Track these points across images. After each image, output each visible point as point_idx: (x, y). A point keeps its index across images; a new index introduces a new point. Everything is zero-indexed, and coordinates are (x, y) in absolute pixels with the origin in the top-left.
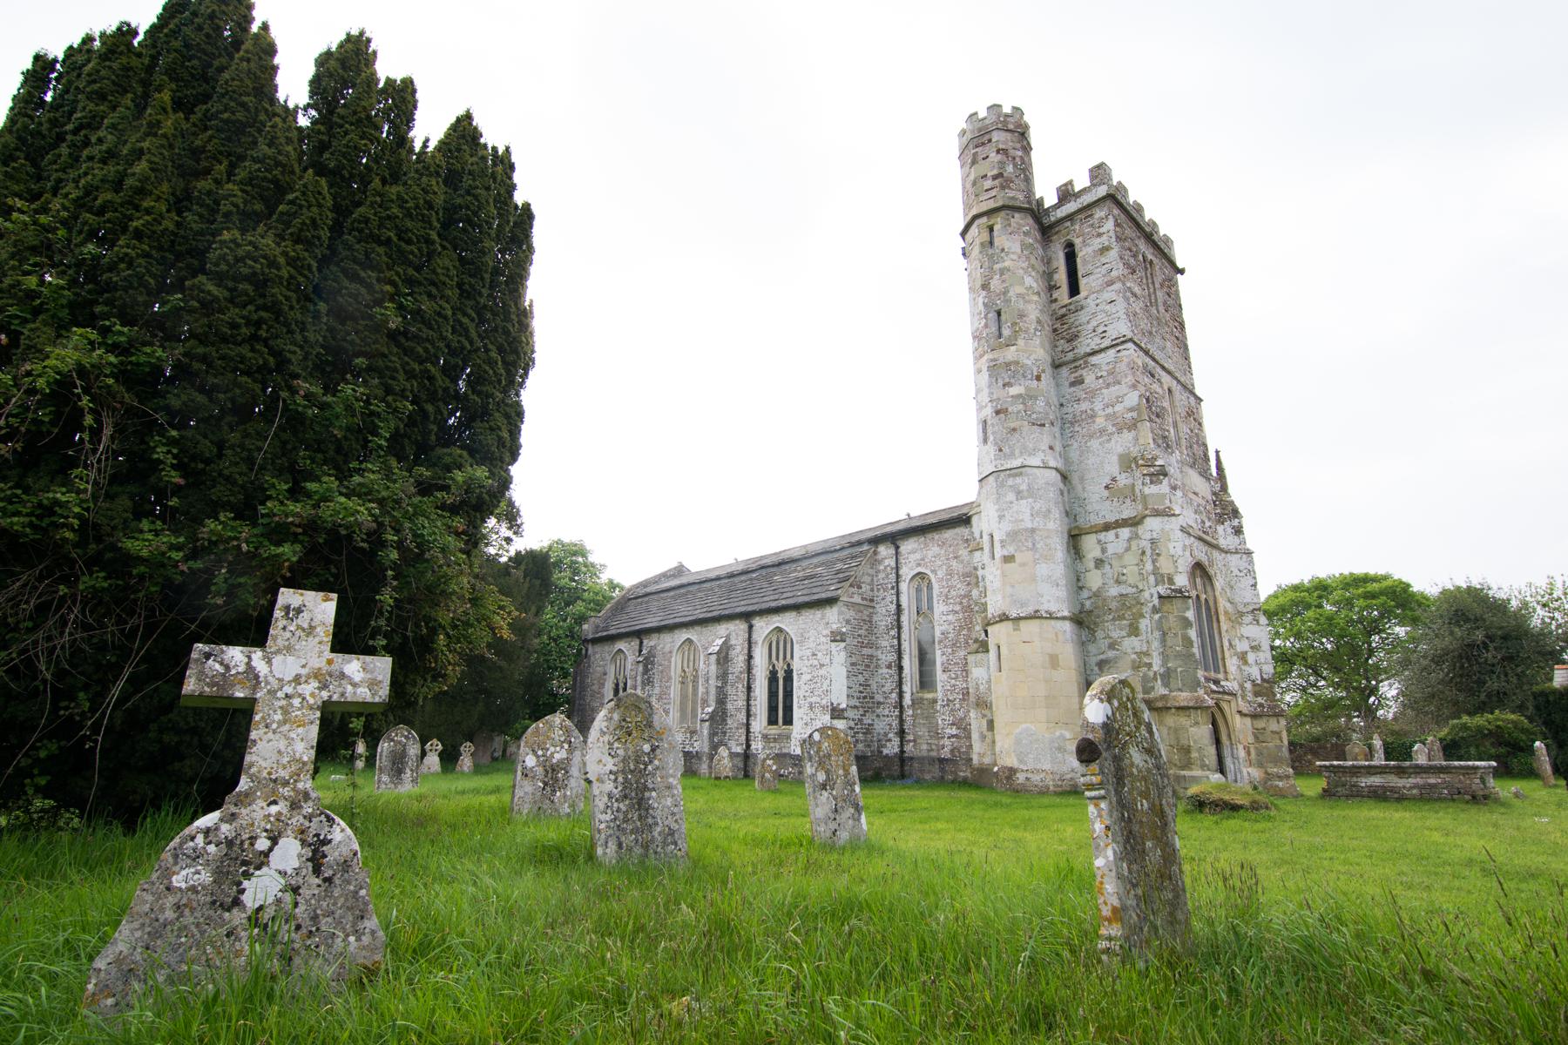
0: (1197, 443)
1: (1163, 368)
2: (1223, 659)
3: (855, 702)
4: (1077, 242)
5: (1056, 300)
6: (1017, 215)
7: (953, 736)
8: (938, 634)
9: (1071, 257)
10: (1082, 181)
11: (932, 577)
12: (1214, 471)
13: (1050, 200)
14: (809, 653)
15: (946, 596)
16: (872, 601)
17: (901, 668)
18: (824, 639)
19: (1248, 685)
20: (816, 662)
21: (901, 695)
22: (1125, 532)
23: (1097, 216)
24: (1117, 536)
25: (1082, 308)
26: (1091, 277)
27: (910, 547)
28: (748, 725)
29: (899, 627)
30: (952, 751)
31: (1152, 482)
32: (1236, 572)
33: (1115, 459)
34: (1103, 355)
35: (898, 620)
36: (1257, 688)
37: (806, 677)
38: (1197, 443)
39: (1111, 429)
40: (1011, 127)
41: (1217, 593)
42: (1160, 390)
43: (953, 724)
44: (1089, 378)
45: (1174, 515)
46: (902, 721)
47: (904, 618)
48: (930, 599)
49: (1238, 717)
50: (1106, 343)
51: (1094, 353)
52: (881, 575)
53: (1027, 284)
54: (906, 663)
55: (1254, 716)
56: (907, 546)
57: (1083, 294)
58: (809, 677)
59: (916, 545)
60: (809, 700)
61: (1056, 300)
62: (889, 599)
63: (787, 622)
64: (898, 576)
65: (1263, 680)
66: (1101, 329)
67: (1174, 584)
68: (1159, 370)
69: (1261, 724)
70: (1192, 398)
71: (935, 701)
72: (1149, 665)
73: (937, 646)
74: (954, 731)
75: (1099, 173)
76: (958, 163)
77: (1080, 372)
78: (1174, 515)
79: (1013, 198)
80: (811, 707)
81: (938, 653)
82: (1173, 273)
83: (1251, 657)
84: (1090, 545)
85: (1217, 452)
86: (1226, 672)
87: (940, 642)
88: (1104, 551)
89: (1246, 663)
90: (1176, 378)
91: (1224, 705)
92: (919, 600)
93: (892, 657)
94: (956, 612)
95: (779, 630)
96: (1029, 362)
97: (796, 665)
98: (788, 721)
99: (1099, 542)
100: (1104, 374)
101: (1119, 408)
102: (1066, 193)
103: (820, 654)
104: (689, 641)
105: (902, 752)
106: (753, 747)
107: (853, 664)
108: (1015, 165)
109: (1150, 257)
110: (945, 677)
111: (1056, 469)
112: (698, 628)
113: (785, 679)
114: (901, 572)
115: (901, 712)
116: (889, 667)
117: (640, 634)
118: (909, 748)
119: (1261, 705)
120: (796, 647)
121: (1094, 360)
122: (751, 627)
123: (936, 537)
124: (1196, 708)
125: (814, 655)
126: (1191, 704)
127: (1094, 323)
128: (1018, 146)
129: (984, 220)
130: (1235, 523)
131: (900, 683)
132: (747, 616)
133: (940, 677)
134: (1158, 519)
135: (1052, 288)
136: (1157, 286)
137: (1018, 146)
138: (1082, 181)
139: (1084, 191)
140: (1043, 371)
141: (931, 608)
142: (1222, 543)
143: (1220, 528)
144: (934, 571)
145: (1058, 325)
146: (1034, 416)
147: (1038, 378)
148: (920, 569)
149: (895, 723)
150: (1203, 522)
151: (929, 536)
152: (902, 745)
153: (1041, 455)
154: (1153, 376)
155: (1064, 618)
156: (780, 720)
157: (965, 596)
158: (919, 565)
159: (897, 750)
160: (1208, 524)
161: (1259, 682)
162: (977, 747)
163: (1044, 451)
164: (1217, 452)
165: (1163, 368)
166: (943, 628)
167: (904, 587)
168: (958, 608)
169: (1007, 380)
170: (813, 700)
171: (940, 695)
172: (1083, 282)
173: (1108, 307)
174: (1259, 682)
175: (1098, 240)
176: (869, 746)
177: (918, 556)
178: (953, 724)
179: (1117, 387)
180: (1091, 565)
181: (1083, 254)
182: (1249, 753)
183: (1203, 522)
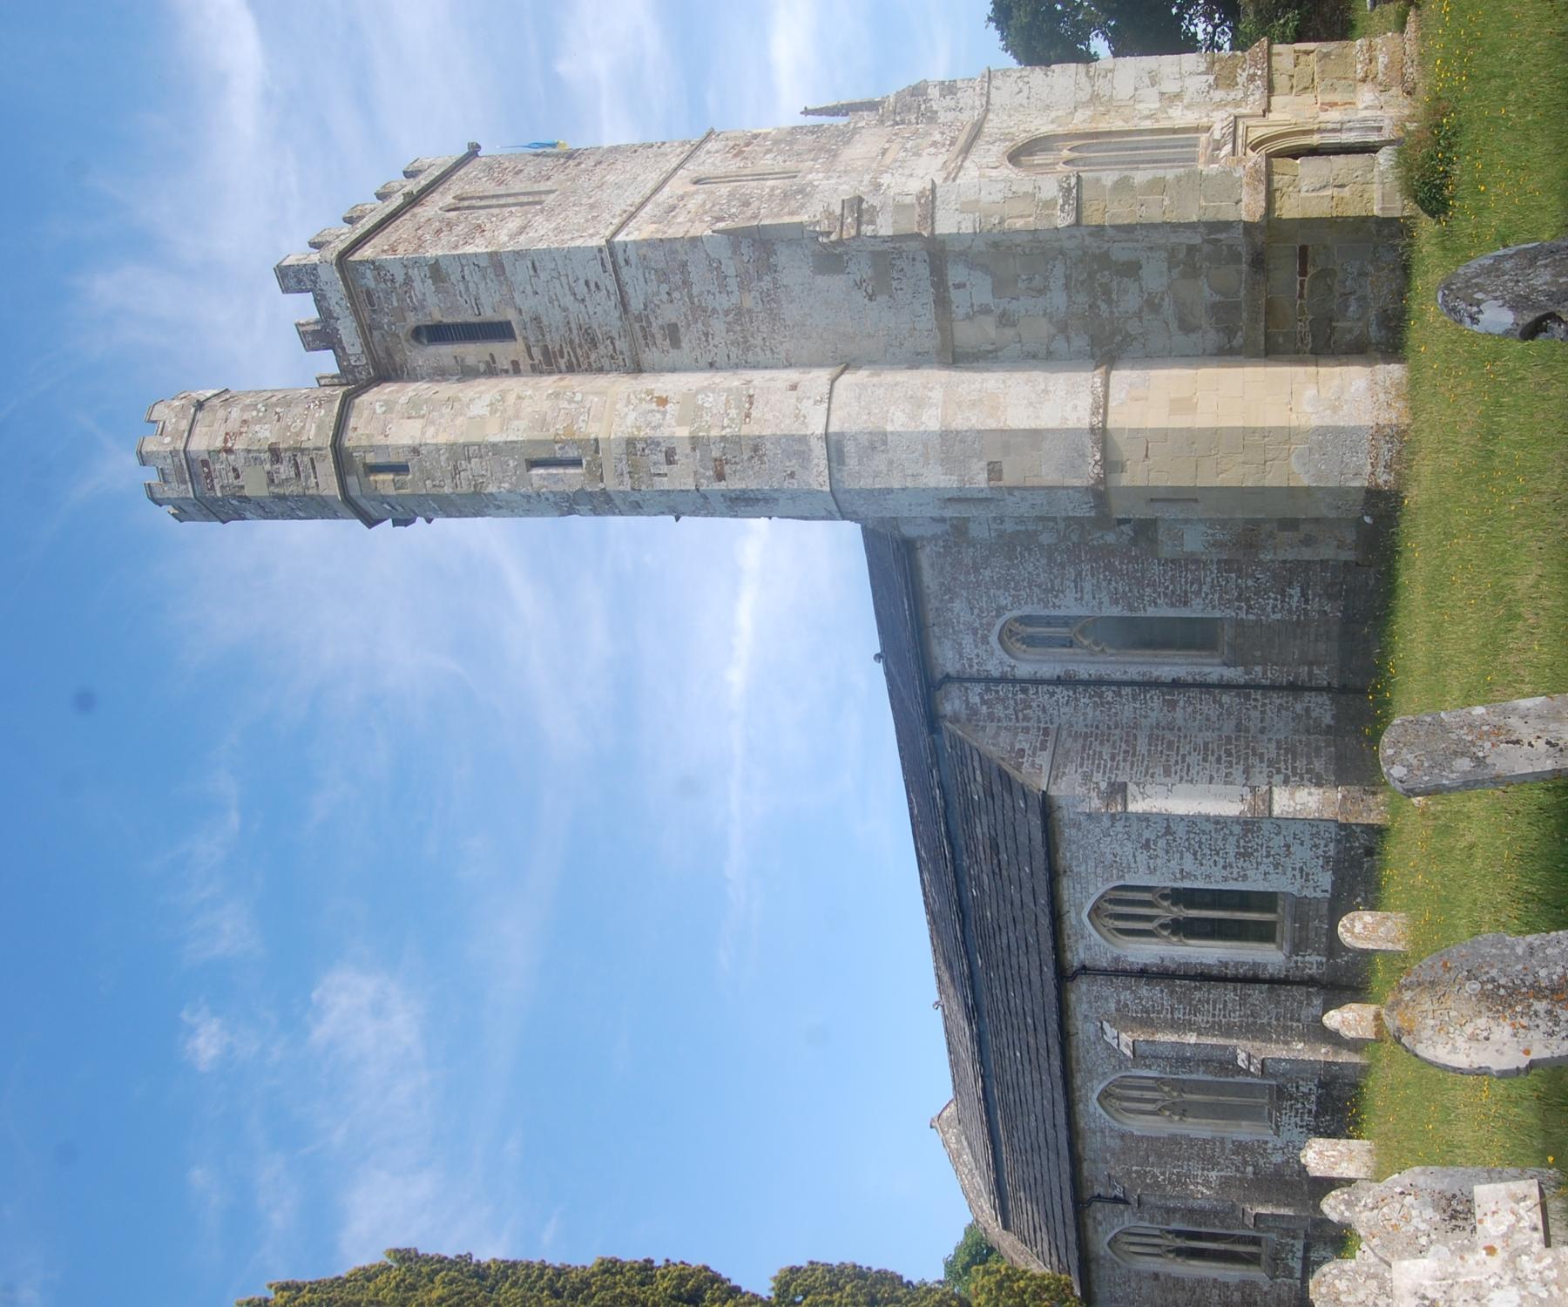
0: (790, 143)
1: (656, 190)
2: (1174, 131)
3: (1237, 771)
4: (413, 320)
5: (515, 364)
6: (352, 422)
7: (1304, 594)
8: (1115, 611)
9: (437, 333)
10: (303, 308)
11: (1008, 615)
12: (840, 121)
13: (327, 362)
14: (1142, 857)
15: (1046, 591)
16: (1046, 732)
17: (1176, 684)
19: (1218, 95)
20: (1162, 843)
21: (1226, 686)
22: (956, 273)
23: (372, 284)
24: (959, 286)
25: (537, 319)
26: (483, 300)
27: (950, 654)
28: (1273, 981)
29: (1099, 682)
30: (1330, 597)
31: (872, 222)
32: (1022, 98)
33: (822, 281)
34: (630, 290)
35: (1087, 683)
37: (1189, 863)
38: (790, 143)
39: (766, 283)
40: (184, 425)
41: (1060, 131)
42: (700, 198)
43: (1283, 594)
44: (669, 314)
45: (933, 191)
46: (1274, 687)
47: (1084, 671)
48: (1048, 622)
49: (1271, 116)
50: (609, 282)
51: (624, 304)
52: (999, 711)
53: (486, 411)
54: (1166, 672)
55: (1270, 89)
56: (946, 658)
57: (511, 315)
58: (1188, 857)
59: (948, 644)
60: (1231, 858)
61: (515, 364)
62: (1044, 699)
63: (1080, 897)
64: (1002, 680)
66: (581, 289)
67: (1054, 200)
68: (660, 197)
69: (1280, 81)
70: (709, 146)
71: (1239, 623)
72: (1191, 249)
73: (1141, 614)
74: (1296, 592)
75: (292, 278)
76: (234, 525)
77: (655, 329)
78: (933, 191)
79: (319, 428)
80: (1245, 855)
81: (1151, 612)
82: (476, 162)
83: (1171, 87)
84: (966, 334)
85: (806, 112)
86: (1197, 129)
87: (1131, 608)
88: (985, 310)
89: (1178, 96)
90: (675, 170)
91: (1254, 135)
92: (1048, 642)
93: (1155, 700)
94: (1079, 574)
95: (1096, 911)
96: (632, 416)
97: (1163, 880)
98: (1267, 901)
99: (969, 317)
100: (665, 288)
101: (730, 269)
102: (320, 337)
103: (1147, 834)
104: (1105, 1095)
105: (1328, 689)
106: (1314, 971)
107: (1167, 773)
108: (259, 421)
109: (449, 200)
110: (1197, 602)
111: (833, 381)
112: (1078, 1081)
113: (1190, 905)
114: (996, 674)
115: (1258, 687)
116: (1172, 705)
117: (1081, 1203)
118: (1322, 675)
119: (1252, 78)
120: (1130, 880)
121: (636, 304)
122: (1084, 969)
123: (932, 604)
124: (1269, 182)
126: (1262, 188)
127: (568, 300)
128: (221, 413)
129: (352, 481)
130: (934, 93)
131: (1205, 686)
132: (1064, 976)
133: (1196, 610)
134: (939, 215)
135: (491, 371)
136: (502, 190)
137: (221, 413)
138: (303, 308)
139: (320, 300)
140: (649, 392)
141: (1066, 622)
142: (969, 117)
143: (943, 117)
144: (1000, 611)
145: (562, 363)
146: (733, 412)
147: (663, 401)
148: (993, 639)
149: (1277, 699)
150: (934, 144)
151: (931, 617)
152: (1318, 689)
153: (807, 405)
154: (673, 208)
155: (1106, 385)
157: (1050, 559)
158: (985, 640)
159: (1324, 699)
160: (937, 137)
161: (1211, 78)
162: (1327, 552)
163: (799, 400)
164: (806, 112)
165: (656, 190)
166: (1106, 600)
167: (1024, 670)
168: (1071, 572)
169: (661, 458)
170: (1231, 850)
171: (1231, 613)
172: (489, 315)
173: (543, 276)
175: (417, 284)
176: (1318, 749)
177: (967, 640)
178: (1283, 594)
179: (691, 268)
180: (1009, 333)
181: (437, 313)
182: (1333, 105)
183: (934, 144)
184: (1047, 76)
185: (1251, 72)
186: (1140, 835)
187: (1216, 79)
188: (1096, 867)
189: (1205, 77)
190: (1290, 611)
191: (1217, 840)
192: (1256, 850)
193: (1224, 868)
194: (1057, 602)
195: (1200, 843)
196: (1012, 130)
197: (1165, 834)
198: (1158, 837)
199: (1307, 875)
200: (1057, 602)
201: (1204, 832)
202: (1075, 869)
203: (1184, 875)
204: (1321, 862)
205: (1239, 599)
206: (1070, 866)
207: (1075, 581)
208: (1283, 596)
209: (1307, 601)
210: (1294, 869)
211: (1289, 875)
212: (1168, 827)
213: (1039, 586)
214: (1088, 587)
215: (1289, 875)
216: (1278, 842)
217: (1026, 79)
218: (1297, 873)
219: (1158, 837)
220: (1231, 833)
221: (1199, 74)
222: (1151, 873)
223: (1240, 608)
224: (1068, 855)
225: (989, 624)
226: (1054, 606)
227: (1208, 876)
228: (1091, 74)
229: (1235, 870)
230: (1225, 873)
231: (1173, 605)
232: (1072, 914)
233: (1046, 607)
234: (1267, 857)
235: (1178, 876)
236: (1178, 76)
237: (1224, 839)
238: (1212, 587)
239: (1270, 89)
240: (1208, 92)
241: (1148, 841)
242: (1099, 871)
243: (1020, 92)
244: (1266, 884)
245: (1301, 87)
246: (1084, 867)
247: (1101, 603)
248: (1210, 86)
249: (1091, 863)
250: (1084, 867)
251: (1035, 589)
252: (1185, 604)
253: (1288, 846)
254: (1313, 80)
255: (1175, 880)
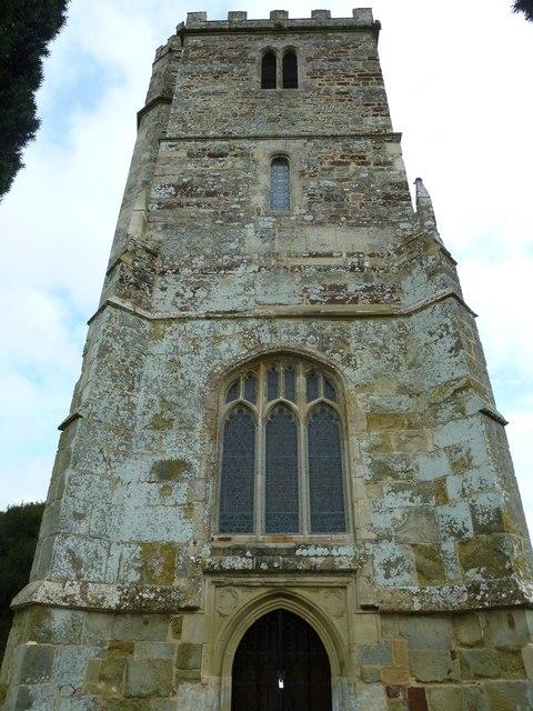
19: (450, 546)
32: (424, 337)
36: (470, 549)
65: (479, 529)
83: (453, 486)
89: (445, 500)
91: (325, 603)
119: (475, 588)
161: (470, 534)
174: (470, 534)
184: (451, 352)
185: (483, 587)
187: (469, 540)
189: (469, 525)
196: (353, 345)
217: (445, 333)
221: (473, 517)
228: (459, 395)
236: (467, 492)
239: (457, 616)
240: (452, 534)
243: (431, 334)
245: (468, 658)
248: (460, 535)
254: (481, 677)
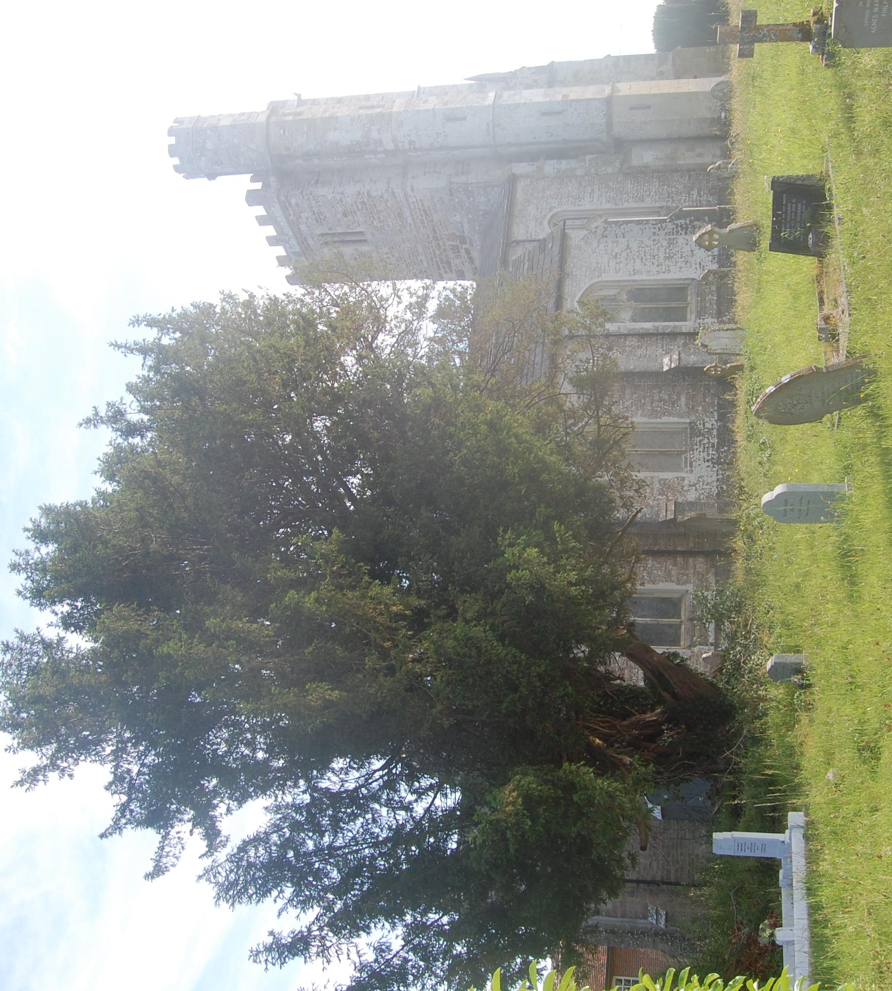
7: (699, 193)
8: (609, 206)
18: (602, 246)
20: (624, 254)
30: (711, 194)
37: (638, 265)
60: (662, 261)
73: (621, 206)
74: (695, 192)
80: (667, 258)
87: (616, 204)
110: (648, 200)
125: (616, 257)
156: (681, 304)
168: (589, 189)
170: (662, 255)
186: (613, 251)
188: (586, 271)
190: (692, 201)
191: (654, 250)
192: (675, 254)
193: (658, 266)
194: (580, 203)
195: (645, 252)
197: (626, 249)
198: (622, 251)
199: (703, 266)
200: (580, 203)
201: (647, 246)
202: (575, 273)
203: (635, 272)
204: (710, 258)
205: (668, 197)
206: (572, 272)
207: (590, 194)
208: (689, 195)
209: (700, 197)
210: (696, 264)
211: (694, 266)
212: (628, 245)
213: (572, 197)
214: (596, 195)
215: (694, 266)
216: (687, 249)
218: (698, 266)
219: (622, 251)
220: (662, 246)
222: (616, 272)
223: (668, 201)
224: (572, 265)
225: (544, 215)
226: (578, 205)
227: (649, 272)
229: (664, 267)
230: (658, 269)
231: (636, 202)
232: (569, 301)
233: (574, 206)
234: (681, 258)
235: (632, 273)
237: (658, 249)
238: (656, 192)
241: (616, 254)
242: (587, 273)
244: (681, 274)
246: (579, 272)
247: (601, 203)
249: (584, 269)
250: (579, 272)
251: (571, 198)
252: (642, 200)
253: (693, 251)
255: (630, 275)
